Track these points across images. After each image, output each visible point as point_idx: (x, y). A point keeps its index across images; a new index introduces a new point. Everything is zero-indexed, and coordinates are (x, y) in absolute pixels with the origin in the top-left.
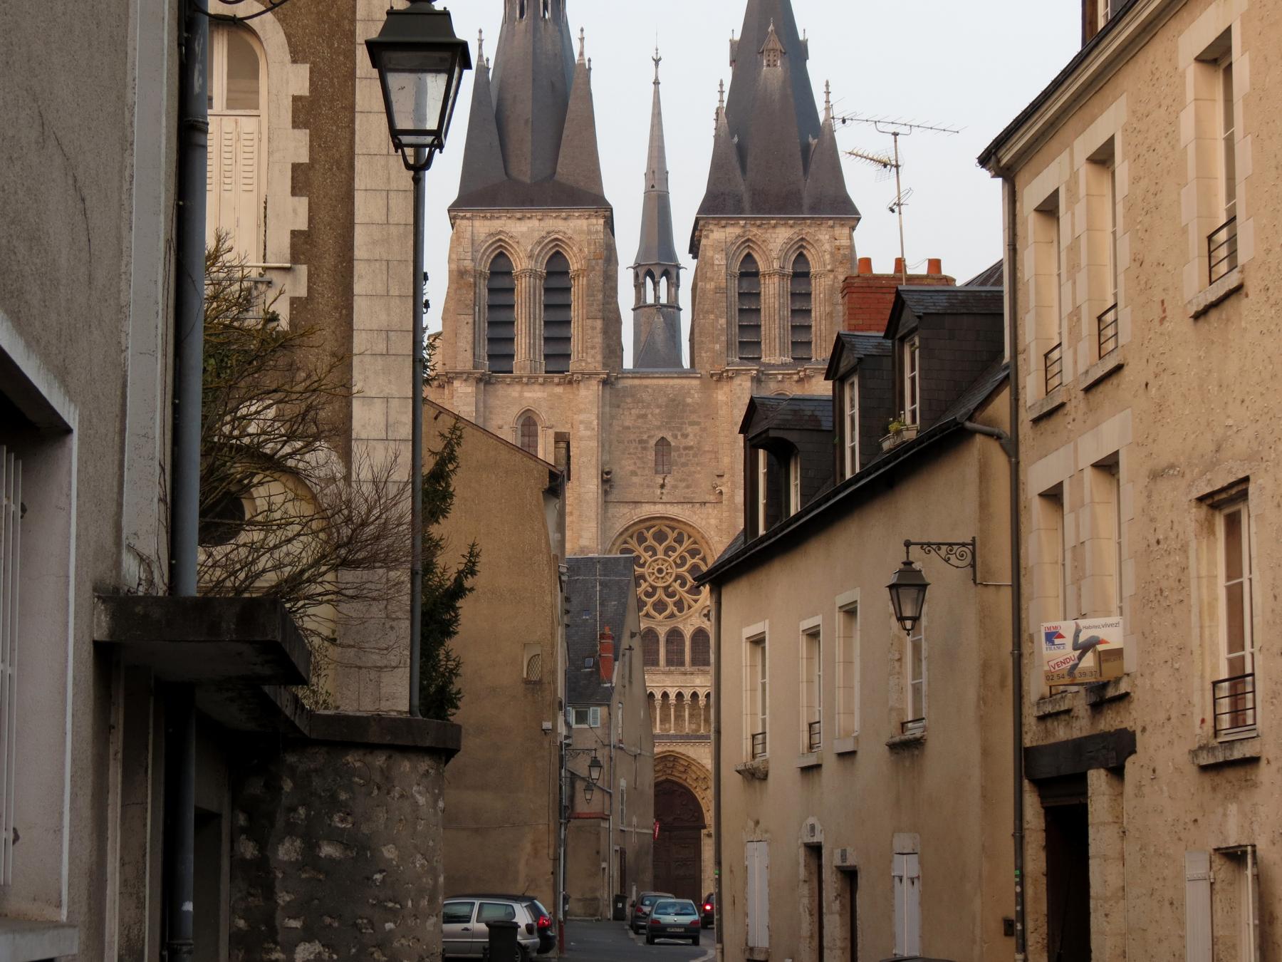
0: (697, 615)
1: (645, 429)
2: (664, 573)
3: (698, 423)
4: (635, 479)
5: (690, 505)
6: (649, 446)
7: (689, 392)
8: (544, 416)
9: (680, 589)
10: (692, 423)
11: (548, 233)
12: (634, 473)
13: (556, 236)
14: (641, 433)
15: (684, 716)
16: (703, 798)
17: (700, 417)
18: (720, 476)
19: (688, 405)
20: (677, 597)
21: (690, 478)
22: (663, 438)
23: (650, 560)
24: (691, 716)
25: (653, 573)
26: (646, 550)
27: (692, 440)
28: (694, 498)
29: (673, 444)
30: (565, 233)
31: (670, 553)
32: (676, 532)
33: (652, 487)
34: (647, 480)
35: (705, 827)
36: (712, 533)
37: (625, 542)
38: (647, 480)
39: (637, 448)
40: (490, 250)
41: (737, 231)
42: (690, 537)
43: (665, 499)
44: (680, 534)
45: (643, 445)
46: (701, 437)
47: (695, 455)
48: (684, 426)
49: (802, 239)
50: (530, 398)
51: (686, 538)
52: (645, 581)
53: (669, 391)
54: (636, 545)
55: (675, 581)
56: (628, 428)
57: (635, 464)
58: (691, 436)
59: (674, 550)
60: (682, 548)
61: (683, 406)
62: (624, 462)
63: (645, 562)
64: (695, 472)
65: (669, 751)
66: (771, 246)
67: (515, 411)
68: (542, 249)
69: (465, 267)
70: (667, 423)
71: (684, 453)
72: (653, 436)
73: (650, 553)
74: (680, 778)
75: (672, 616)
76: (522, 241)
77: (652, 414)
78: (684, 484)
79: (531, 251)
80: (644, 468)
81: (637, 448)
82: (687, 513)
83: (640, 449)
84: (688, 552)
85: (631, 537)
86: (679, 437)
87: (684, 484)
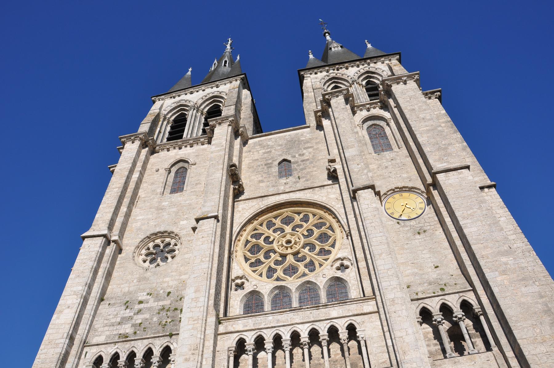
0: (329, 267)
2: (293, 242)
3: (311, 147)
4: (261, 184)
5: (311, 190)
7: (302, 135)
8: (191, 161)
9: (310, 253)
10: (305, 148)
11: (209, 94)
12: (261, 181)
13: (213, 95)
14: (266, 160)
18: (333, 161)
19: (302, 141)
20: (308, 260)
21: (308, 176)
23: (278, 237)
25: (282, 246)
26: (274, 231)
27: (307, 156)
30: (218, 91)
31: (297, 229)
32: (301, 216)
33: (277, 186)
34: (272, 183)
36: (333, 203)
37: (255, 229)
38: (272, 183)
39: (264, 168)
40: (175, 111)
41: (324, 73)
42: (314, 215)
43: (287, 191)
46: (314, 153)
47: (312, 162)
48: (301, 151)
49: (367, 72)
50: (183, 154)
51: (311, 216)
52: (275, 252)
54: (266, 229)
55: (303, 247)
56: (258, 159)
57: (262, 176)
58: (307, 154)
59: (301, 226)
60: (308, 224)
61: (299, 141)
62: (253, 178)
63: (274, 239)
66: (349, 74)
68: (204, 102)
70: (286, 152)
71: (302, 163)
73: (279, 232)
75: (304, 275)
77: (275, 150)
78: (304, 179)
79: (197, 101)
80: (269, 177)
81: (264, 168)
84: (314, 226)
85: (261, 225)
86: (297, 156)
87: (304, 179)
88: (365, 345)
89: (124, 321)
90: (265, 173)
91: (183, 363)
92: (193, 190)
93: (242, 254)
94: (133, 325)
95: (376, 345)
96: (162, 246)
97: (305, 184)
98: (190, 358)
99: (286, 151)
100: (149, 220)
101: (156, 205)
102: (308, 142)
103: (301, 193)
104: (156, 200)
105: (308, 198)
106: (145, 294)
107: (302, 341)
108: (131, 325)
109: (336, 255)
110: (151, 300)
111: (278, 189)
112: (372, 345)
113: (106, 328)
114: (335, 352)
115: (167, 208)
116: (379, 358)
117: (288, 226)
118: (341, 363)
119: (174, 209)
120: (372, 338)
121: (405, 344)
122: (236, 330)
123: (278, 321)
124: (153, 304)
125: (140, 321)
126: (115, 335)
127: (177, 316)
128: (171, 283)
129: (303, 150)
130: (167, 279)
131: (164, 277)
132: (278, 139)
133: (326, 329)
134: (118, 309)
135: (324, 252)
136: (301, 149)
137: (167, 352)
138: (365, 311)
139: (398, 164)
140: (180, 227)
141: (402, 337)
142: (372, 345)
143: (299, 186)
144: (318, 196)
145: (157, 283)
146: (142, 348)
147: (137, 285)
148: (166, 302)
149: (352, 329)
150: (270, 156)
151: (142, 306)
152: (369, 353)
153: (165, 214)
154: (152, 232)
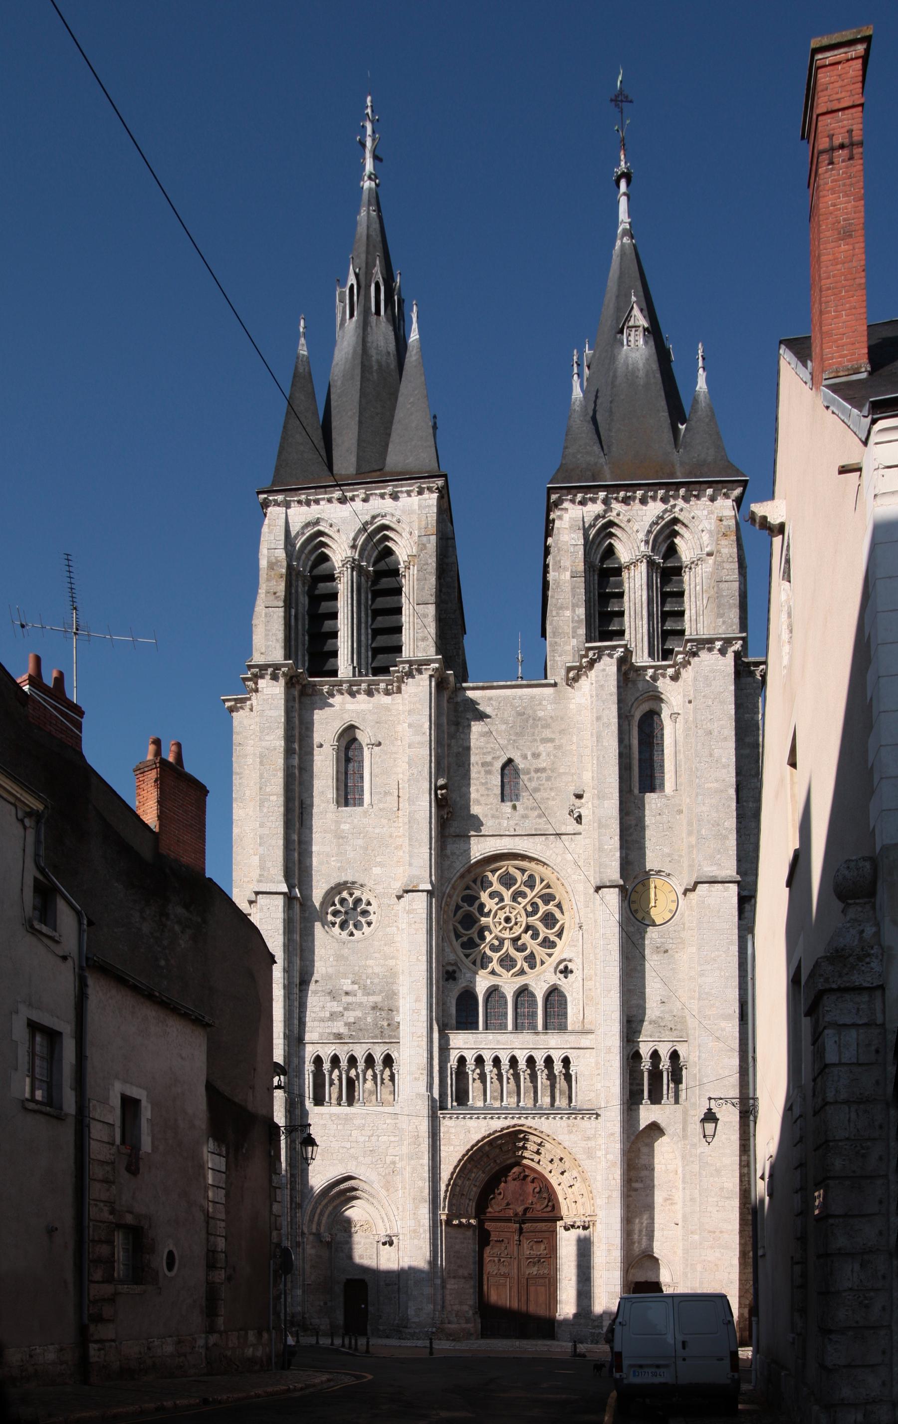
1: (489, 750)
3: (551, 740)
5: (544, 837)
6: (493, 768)
14: (484, 754)
17: (553, 732)
19: (540, 719)
22: (510, 761)
27: (544, 761)
28: (547, 829)
29: (521, 766)
33: (498, 818)
34: (491, 809)
39: (479, 773)
44: (531, 877)
45: (487, 769)
47: (548, 779)
50: (353, 711)
53: (517, 702)
61: (534, 719)
64: (548, 799)
67: (337, 726)
69: (276, 557)
71: (536, 776)
72: (499, 757)
74: (532, 1160)
76: (342, 528)
77: (497, 730)
78: (536, 813)
82: (539, 847)
83: (483, 773)
87: (536, 813)
89: (333, 1016)
90: (482, 784)
92: (381, 806)
93: (451, 928)
94: (347, 1024)
96: (350, 900)
97: (536, 824)
99: (513, 738)
100: (328, 855)
101: (333, 828)
102: (547, 726)
103: (530, 840)
104: (330, 816)
105: (538, 853)
106: (349, 981)
107: (520, 1067)
108: (343, 1023)
109: (562, 952)
110: (360, 993)
111: (500, 824)
113: (316, 1023)
115: (350, 836)
117: (508, 890)
119: (360, 842)
122: (457, 1046)
123: (498, 1042)
124: (360, 998)
125: (352, 1020)
126: (329, 1034)
127: (393, 1019)
128: (377, 970)
129: (539, 743)
130: (370, 962)
131: (366, 959)
132: (502, 704)
133: (543, 1059)
134: (322, 999)
135: (548, 944)
136: (535, 740)
137: (388, 1061)
138: (582, 1046)
139: (663, 824)
140: (373, 878)
143: (528, 826)
144: (551, 851)
145: (359, 966)
146: (362, 1053)
147: (336, 966)
148: (377, 999)
149: (566, 1061)
150: (488, 746)
151: (349, 999)
153: (348, 848)
154: (337, 881)
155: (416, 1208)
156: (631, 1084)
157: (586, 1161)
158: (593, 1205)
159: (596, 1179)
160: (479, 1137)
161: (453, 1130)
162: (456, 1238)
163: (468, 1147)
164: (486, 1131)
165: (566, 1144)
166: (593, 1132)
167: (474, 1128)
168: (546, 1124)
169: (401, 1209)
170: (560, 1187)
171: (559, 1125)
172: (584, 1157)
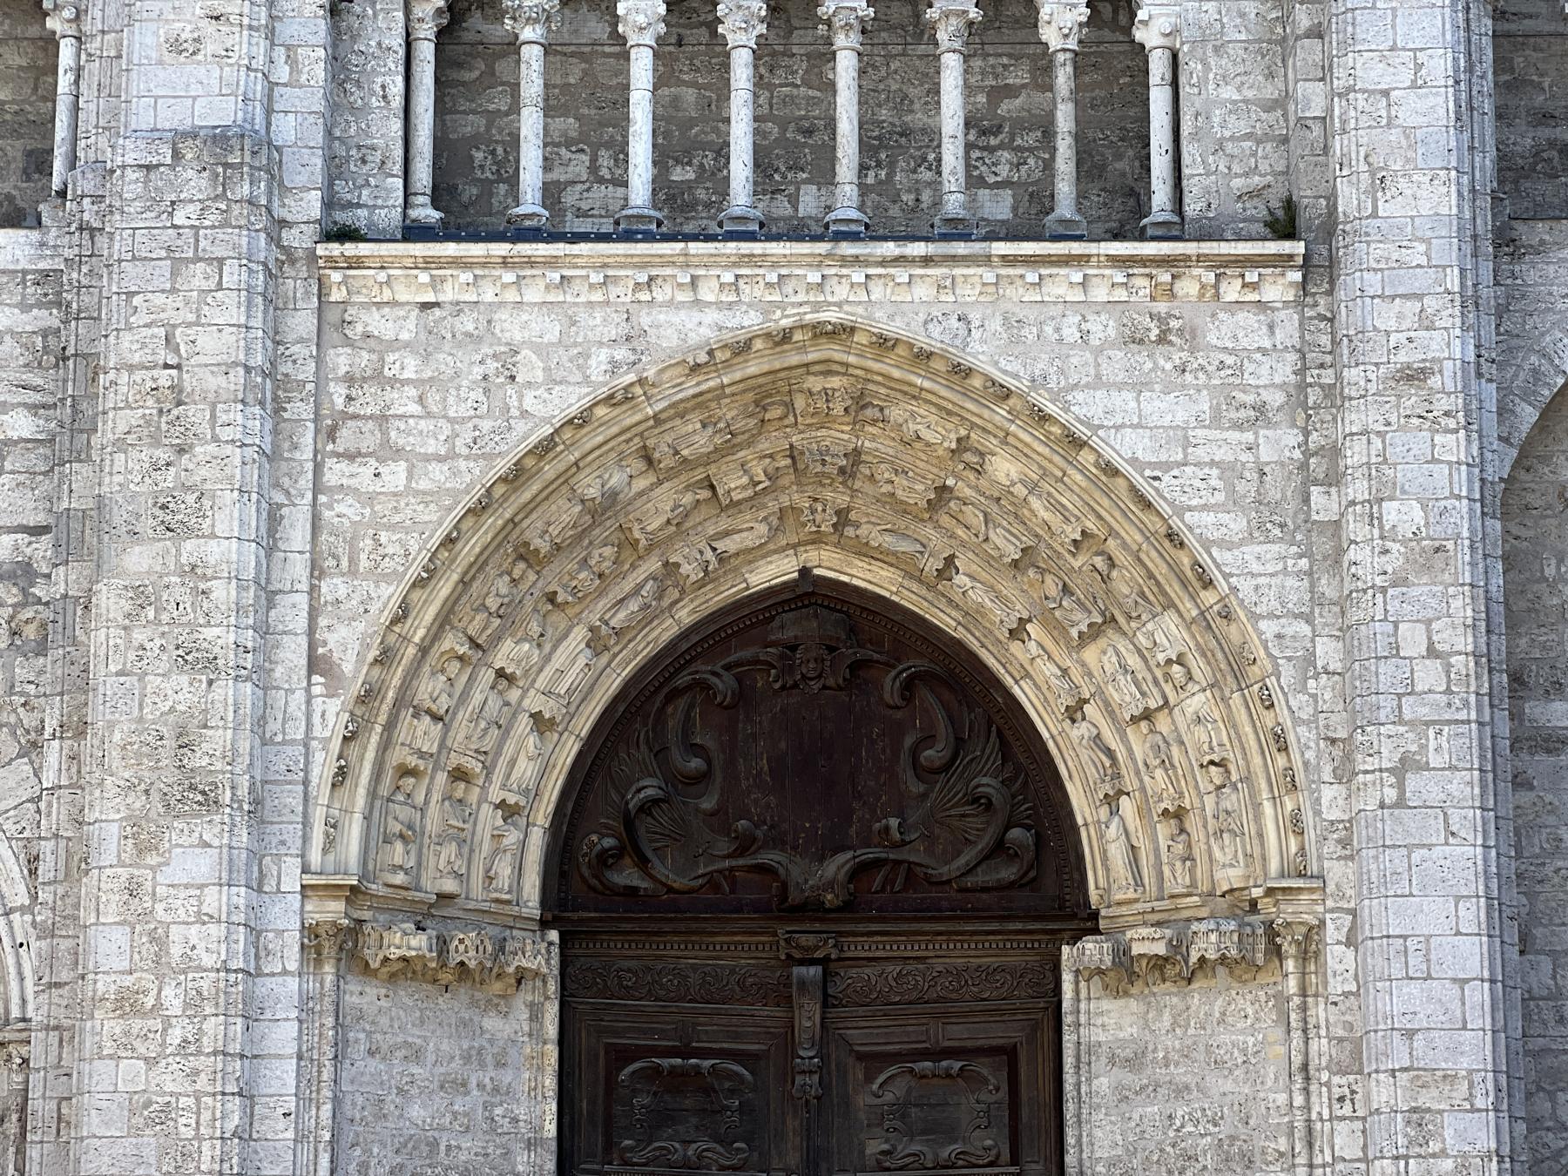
15: (933, 137)
16: (1074, 713)
24: (979, 127)
35: (1086, 922)
65: (821, 332)
88: (1168, 76)
91: (160, 63)
95: (1229, 93)
98: (197, 40)
112: (1211, 86)
114: (996, 77)
116: (1236, 169)
118: (1019, 142)
120: (1216, 49)
121: (1394, 135)
141: (1386, 93)
142: (1211, 86)
152: (1186, 129)
155: (141, 851)
156: (1502, 115)
157: (1251, 551)
158: (1296, 824)
159: (1310, 658)
160: (572, 400)
161: (410, 367)
162: (417, 1055)
163: (502, 466)
164: (614, 365)
165: (1124, 447)
166: (1285, 371)
167: (538, 349)
168: (995, 324)
169: (45, 870)
170: (1082, 730)
171: (1071, 333)
172: (1236, 524)
